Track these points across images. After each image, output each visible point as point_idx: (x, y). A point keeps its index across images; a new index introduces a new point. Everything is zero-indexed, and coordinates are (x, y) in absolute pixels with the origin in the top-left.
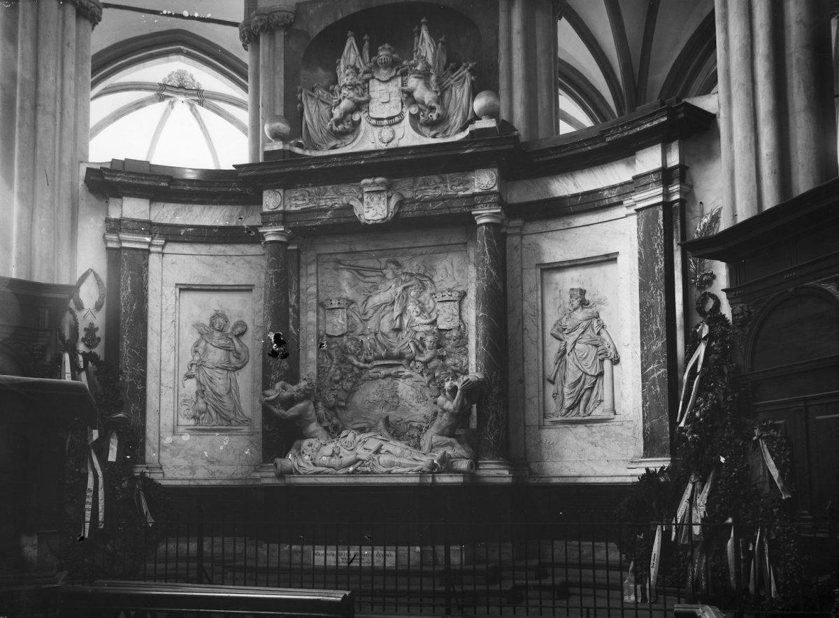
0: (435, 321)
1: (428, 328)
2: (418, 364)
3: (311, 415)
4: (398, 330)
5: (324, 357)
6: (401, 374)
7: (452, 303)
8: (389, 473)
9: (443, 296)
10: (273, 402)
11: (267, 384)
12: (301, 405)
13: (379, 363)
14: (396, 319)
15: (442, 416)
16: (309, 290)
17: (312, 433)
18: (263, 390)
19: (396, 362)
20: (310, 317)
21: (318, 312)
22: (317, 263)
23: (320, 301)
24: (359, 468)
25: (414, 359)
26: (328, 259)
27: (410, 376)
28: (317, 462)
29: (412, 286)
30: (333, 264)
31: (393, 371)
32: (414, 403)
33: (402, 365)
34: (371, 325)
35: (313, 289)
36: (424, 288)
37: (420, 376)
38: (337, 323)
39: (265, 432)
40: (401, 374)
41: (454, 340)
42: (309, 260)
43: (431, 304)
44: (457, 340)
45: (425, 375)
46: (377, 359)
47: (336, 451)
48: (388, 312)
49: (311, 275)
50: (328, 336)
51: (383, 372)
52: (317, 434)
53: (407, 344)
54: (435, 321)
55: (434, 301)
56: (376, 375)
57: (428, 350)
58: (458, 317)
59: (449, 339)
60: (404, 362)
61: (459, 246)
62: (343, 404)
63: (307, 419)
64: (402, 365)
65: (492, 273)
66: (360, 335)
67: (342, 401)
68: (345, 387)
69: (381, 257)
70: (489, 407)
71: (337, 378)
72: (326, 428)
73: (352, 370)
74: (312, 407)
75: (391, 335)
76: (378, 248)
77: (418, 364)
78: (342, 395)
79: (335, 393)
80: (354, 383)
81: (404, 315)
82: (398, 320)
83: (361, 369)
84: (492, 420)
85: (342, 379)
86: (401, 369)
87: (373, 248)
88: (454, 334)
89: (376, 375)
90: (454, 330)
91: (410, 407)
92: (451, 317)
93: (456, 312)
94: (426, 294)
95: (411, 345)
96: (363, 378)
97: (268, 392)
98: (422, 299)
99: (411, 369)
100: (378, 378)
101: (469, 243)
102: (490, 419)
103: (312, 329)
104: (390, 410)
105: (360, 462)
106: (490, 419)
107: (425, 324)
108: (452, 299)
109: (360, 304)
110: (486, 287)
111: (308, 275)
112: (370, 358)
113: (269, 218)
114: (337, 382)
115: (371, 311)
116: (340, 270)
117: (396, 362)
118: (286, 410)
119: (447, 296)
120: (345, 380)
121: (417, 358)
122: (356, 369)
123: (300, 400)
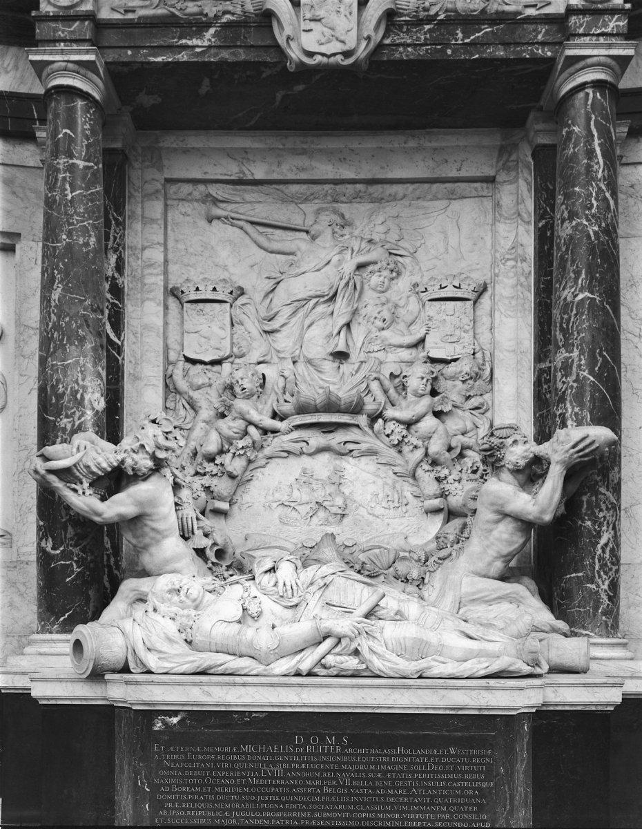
0: (422, 341)
1: (406, 354)
2: (391, 426)
3: (165, 518)
4: (341, 356)
5: (180, 406)
6: (350, 446)
7: (459, 303)
8: (420, 677)
9: (441, 288)
10: (65, 474)
11: (47, 434)
12: (141, 490)
13: (309, 419)
14: (339, 333)
15: (491, 531)
16: (147, 253)
17: (167, 562)
18: (39, 449)
19: (345, 419)
20: (145, 316)
21: (166, 307)
22: (166, 198)
23: (170, 286)
24: (330, 660)
25: (380, 415)
26: (190, 194)
27: (371, 453)
28: (198, 639)
29: (375, 263)
30: (201, 208)
31: (336, 439)
32: (379, 510)
33: (358, 426)
34: (284, 341)
35: (156, 255)
36: (397, 273)
37: (393, 452)
38: (207, 333)
39: (44, 559)
40: (350, 446)
41: (464, 382)
42: (149, 188)
43: (414, 305)
44: (471, 382)
45: (406, 449)
46: (302, 409)
47: (253, 609)
48: (322, 316)
49: (153, 221)
50: (188, 360)
51: (316, 439)
52: (178, 565)
53: (364, 386)
54: (422, 341)
55: (420, 300)
56: (298, 446)
57: (411, 398)
58: (471, 333)
59: (453, 378)
60: (362, 420)
61: (477, 185)
62: (224, 506)
63: (154, 525)
64: (358, 426)
65: (605, 199)
66: (259, 363)
67: (222, 499)
68: (229, 469)
69: (306, 200)
70: (601, 515)
71: (212, 446)
72: (200, 552)
73: (246, 433)
74: (168, 497)
75: (329, 366)
76: (303, 176)
77: (391, 426)
78: (222, 486)
79: (206, 481)
80: (250, 462)
81: (354, 327)
82: (342, 333)
83: (265, 431)
84: (606, 545)
85: (221, 452)
86: (353, 435)
87: (290, 176)
88: (465, 366)
89: (296, 447)
90: (466, 361)
91: (371, 518)
92: (457, 332)
93: (466, 320)
94: (403, 284)
95: (375, 386)
96: (267, 451)
97: (49, 450)
98: (392, 295)
99: (377, 436)
100: (302, 453)
101: (499, 179)
102: (603, 541)
103: (154, 343)
104: (327, 523)
105: (328, 643)
106: (603, 541)
107: (401, 346)
108: (459, 295)
109: (258, 297)
110: (595, 233)
111: (147, 221)
112: (287, 408)
113: (56, 30)
114: (211, 459)
115: (287, 311)
116: (215, 222)
117: (345, 419)
118: (103, 499)
119: (450, 288)
120: (230, 455)
121: (390, 413)
122: (252, 430)
123: (137, 477)
